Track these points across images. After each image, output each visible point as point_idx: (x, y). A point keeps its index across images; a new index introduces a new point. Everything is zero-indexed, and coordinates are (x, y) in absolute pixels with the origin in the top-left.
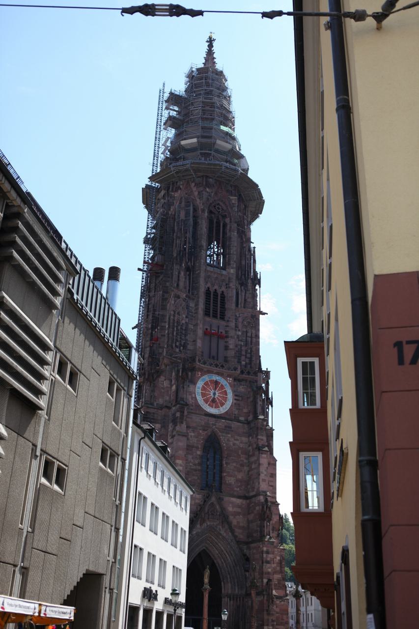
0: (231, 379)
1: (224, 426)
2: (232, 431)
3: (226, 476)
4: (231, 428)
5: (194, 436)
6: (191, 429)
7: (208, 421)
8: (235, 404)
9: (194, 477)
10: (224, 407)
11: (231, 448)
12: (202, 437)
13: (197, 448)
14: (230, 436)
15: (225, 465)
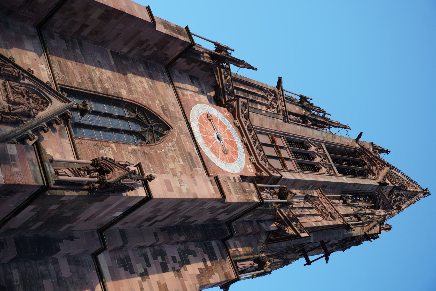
0: (252, 171)
1: (189, 151)
2: (191, 169)
3: (112, 148)
4: (195, 166)
5: (145, 88)
6: (151, 83)
7: (180, 120)
8: (229, 178)
9: (77, 74)
10: (214, 156)
11: (163, 164)
12: (150, 103)
13: (130, 91)
14: (182, 163)
15: (130, 148)
